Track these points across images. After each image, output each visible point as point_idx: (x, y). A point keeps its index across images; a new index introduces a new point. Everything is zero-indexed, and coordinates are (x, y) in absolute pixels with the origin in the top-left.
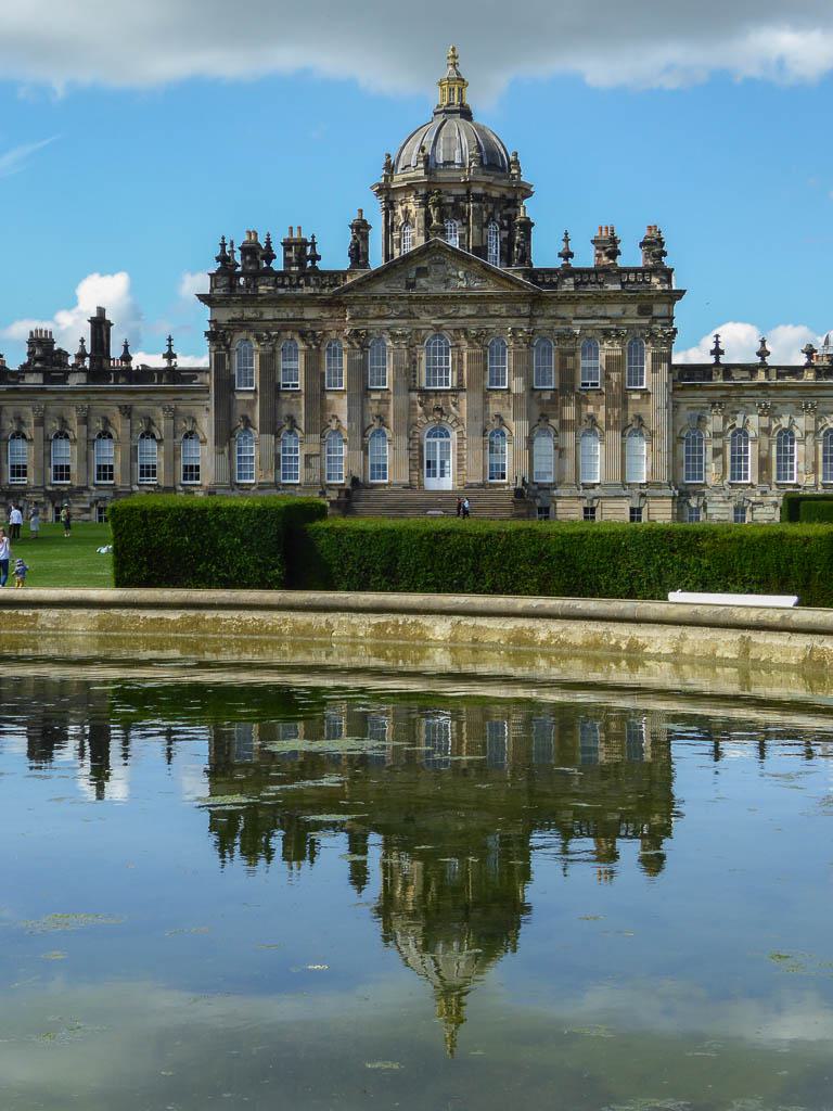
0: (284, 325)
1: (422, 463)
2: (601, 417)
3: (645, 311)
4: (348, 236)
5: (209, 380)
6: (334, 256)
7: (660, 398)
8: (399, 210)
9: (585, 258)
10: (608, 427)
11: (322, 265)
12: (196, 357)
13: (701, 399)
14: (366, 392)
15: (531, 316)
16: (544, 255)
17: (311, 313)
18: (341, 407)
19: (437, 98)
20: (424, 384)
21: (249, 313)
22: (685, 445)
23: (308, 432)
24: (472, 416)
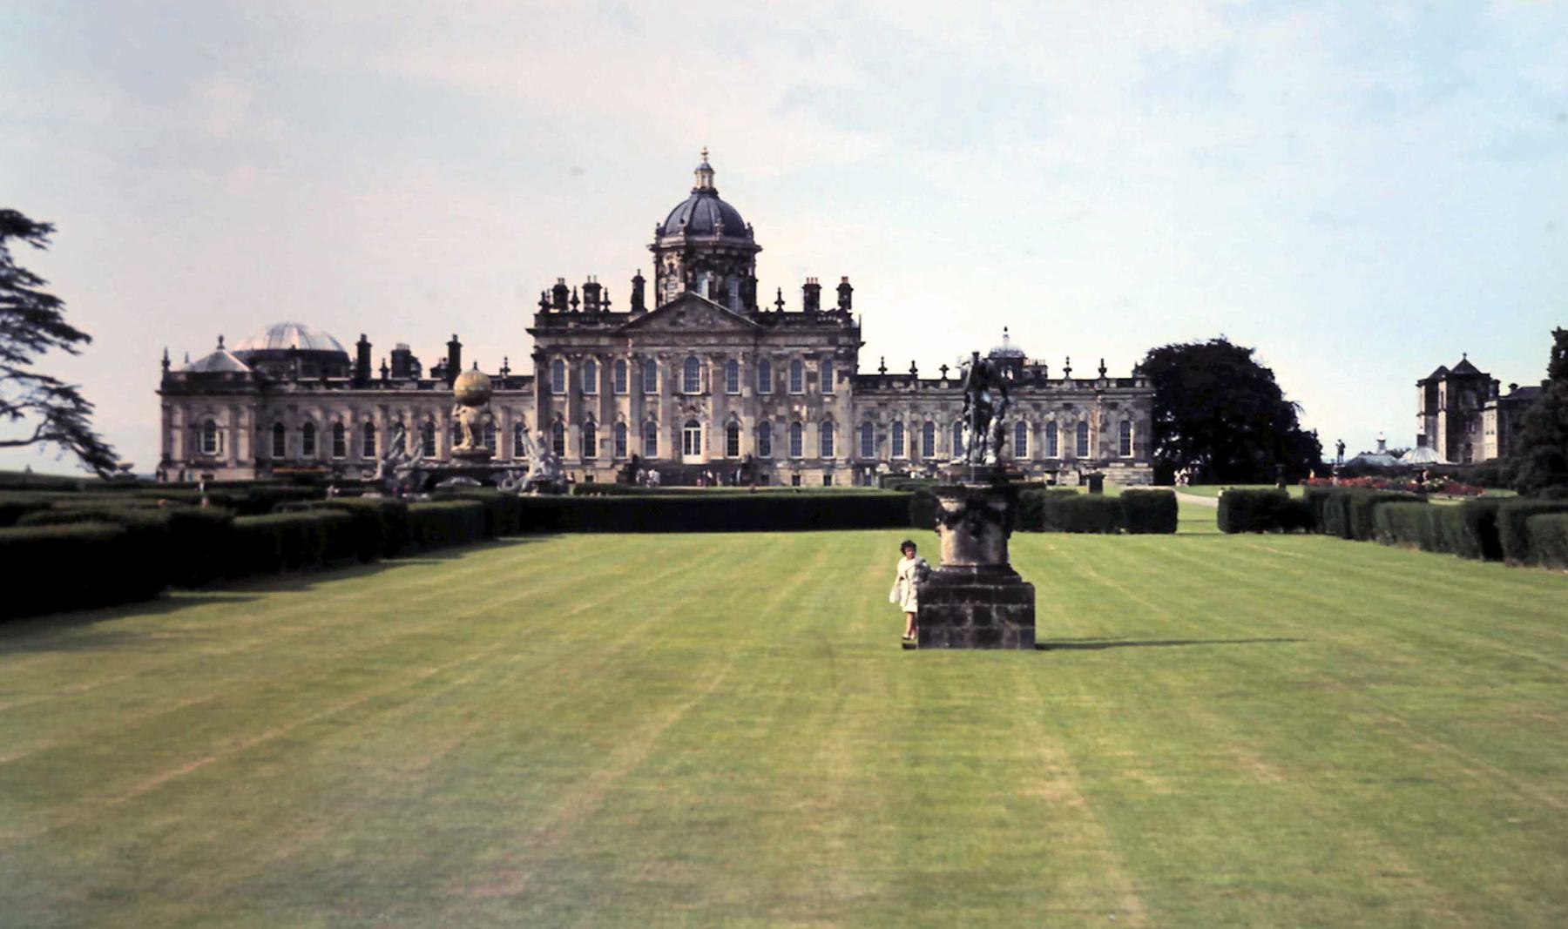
0: (585, 349)
1: (685, 442)
2: (804, 413)
3: (832, 342)
4: (629, 290)
5: (535, 386)
6: (620, 303)
7: (842, 403)
8: (666, 262)
9: (795, 304)
10: (808, 420)
11: (612, 309)
12: (524, 366)
13: (872, 402)
14: (642, 396)
15: (756, 345)
16: (765, 302)
17: (604, 341)
18: (625, 405)
19: (694, 182)
20: (682, 390)
21: (562, 342)
22: (866, 430)
24: (715, 413)
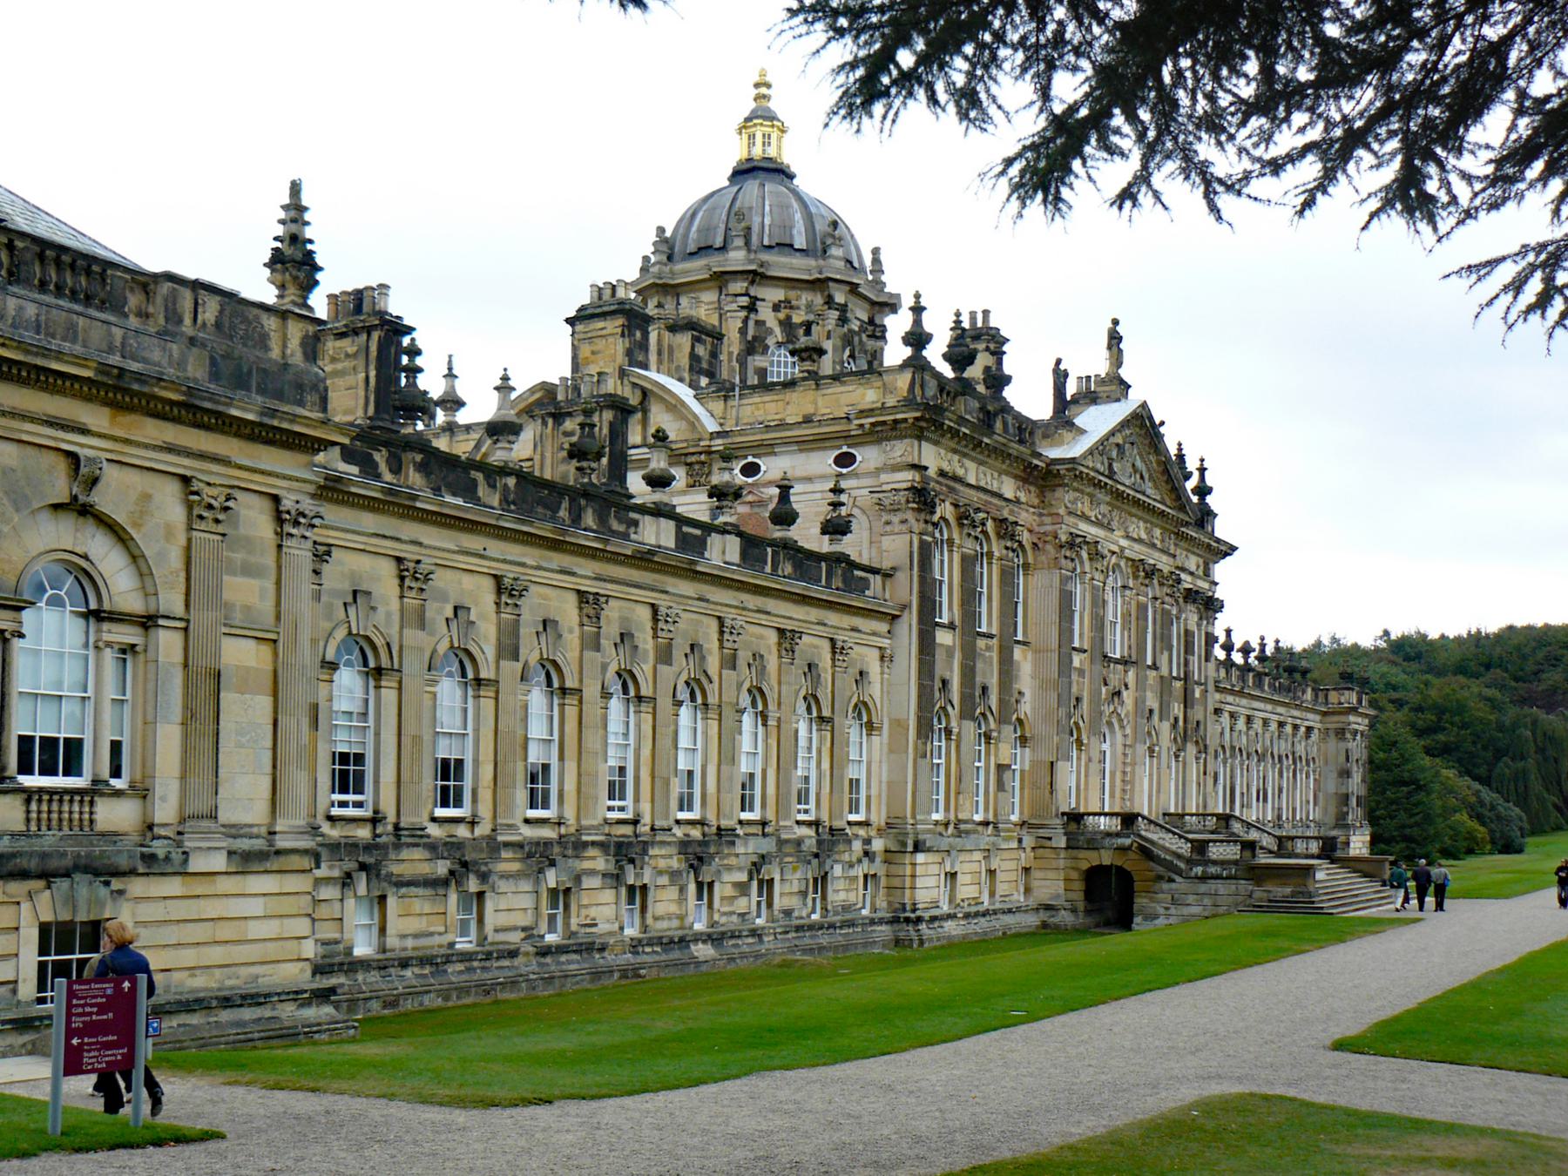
5: (905, 589)
8: (766, 313)
23: (1002, 720)
